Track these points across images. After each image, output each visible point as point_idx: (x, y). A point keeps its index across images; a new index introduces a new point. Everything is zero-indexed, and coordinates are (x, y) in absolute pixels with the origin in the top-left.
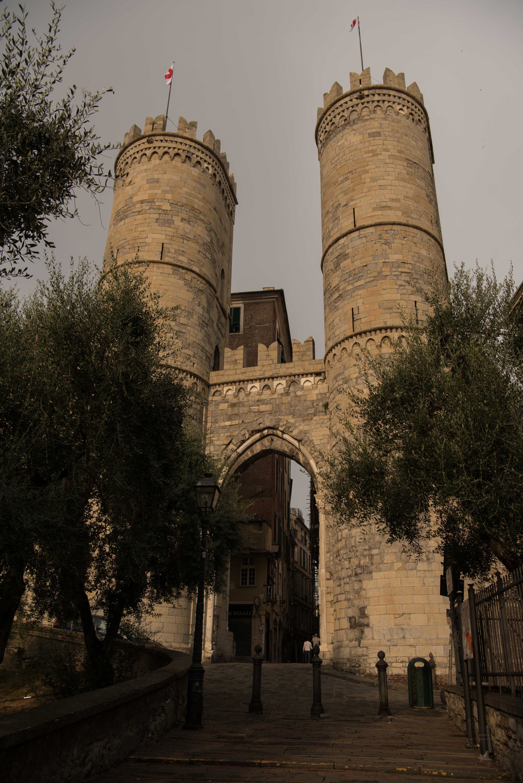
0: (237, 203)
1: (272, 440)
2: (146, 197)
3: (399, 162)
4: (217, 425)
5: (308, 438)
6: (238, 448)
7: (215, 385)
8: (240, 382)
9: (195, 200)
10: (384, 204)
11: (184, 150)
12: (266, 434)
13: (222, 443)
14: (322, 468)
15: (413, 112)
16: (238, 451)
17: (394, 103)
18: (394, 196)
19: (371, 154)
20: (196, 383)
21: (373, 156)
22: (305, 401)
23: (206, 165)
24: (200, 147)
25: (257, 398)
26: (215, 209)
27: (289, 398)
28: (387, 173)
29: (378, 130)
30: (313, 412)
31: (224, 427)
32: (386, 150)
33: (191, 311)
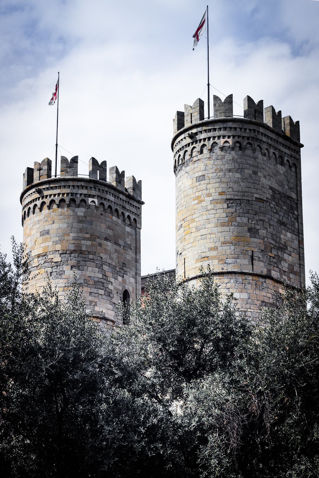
2: (40, 251)
3: (219, 206)
9: (83, 242)
10: (204, 255)
11: (68, 194)
15: (239, 140)
17: (219, 137)
18: (213, 245)
19: (196, 202)
21: (198, 203)
23: (90, 200)
24: (83, 184)
26: (106, 239)
28: (208, 221)
29: (204, 173)
32: (209, 195)
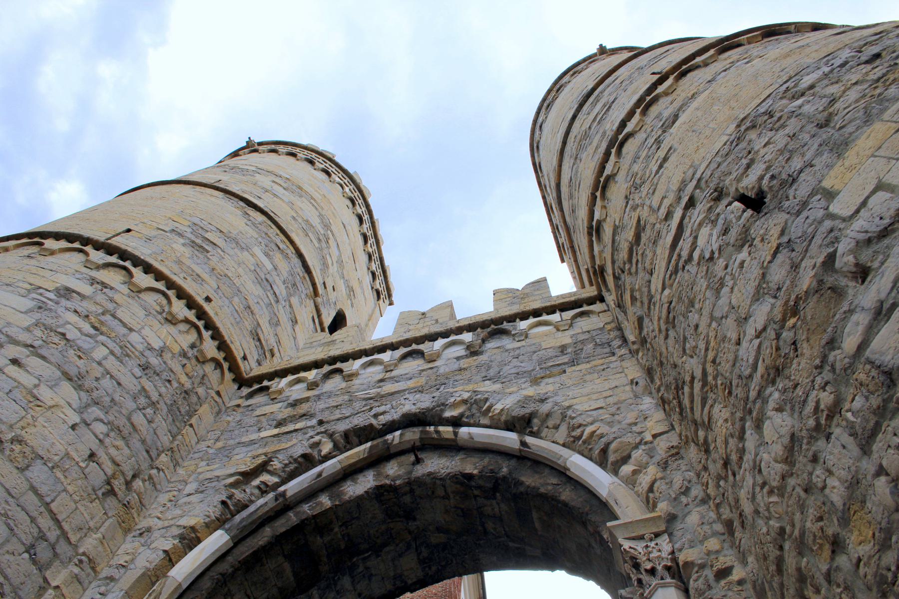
0: (391, 304)
1: (418, 461)
4: (231, 442)
5: (556, 404)
6: (284, 482)
7: (259, 379)
8: (333, 360)
12: (397, 441)
13: (232, 471)
14: (625, 459)
16: (282, 489)
20: (197, 328)
22: (535, 352)
23: (338, 179)
25: (380, 377)
27: (483, 358)
30: (566, 360)
31: (252, 442)
33: (243, 246)
